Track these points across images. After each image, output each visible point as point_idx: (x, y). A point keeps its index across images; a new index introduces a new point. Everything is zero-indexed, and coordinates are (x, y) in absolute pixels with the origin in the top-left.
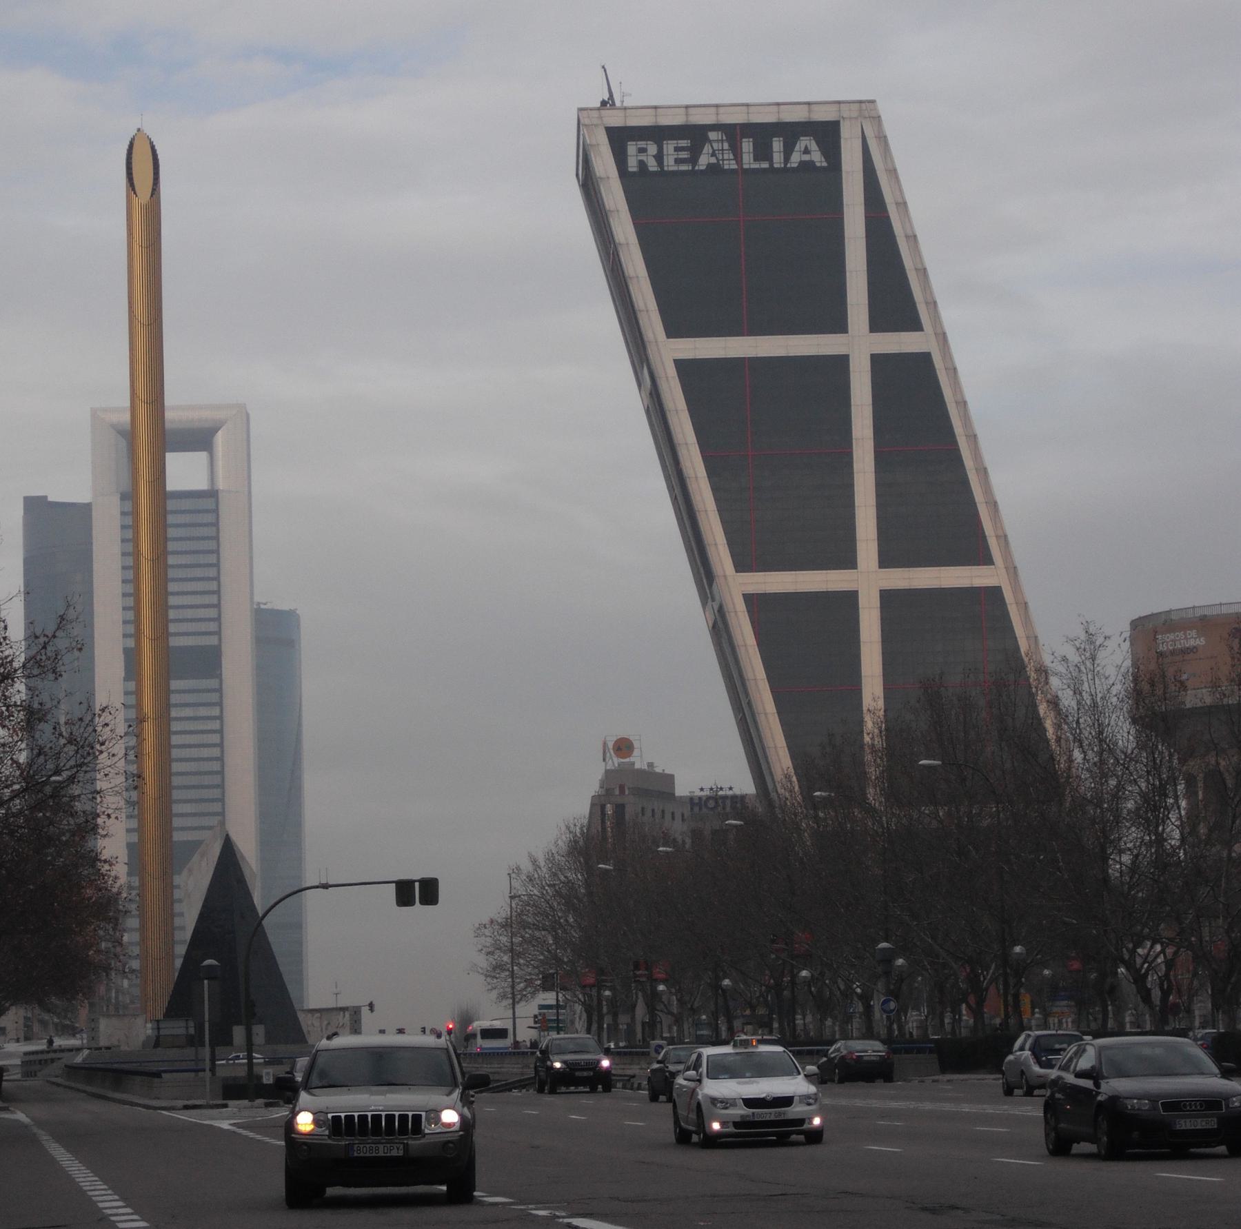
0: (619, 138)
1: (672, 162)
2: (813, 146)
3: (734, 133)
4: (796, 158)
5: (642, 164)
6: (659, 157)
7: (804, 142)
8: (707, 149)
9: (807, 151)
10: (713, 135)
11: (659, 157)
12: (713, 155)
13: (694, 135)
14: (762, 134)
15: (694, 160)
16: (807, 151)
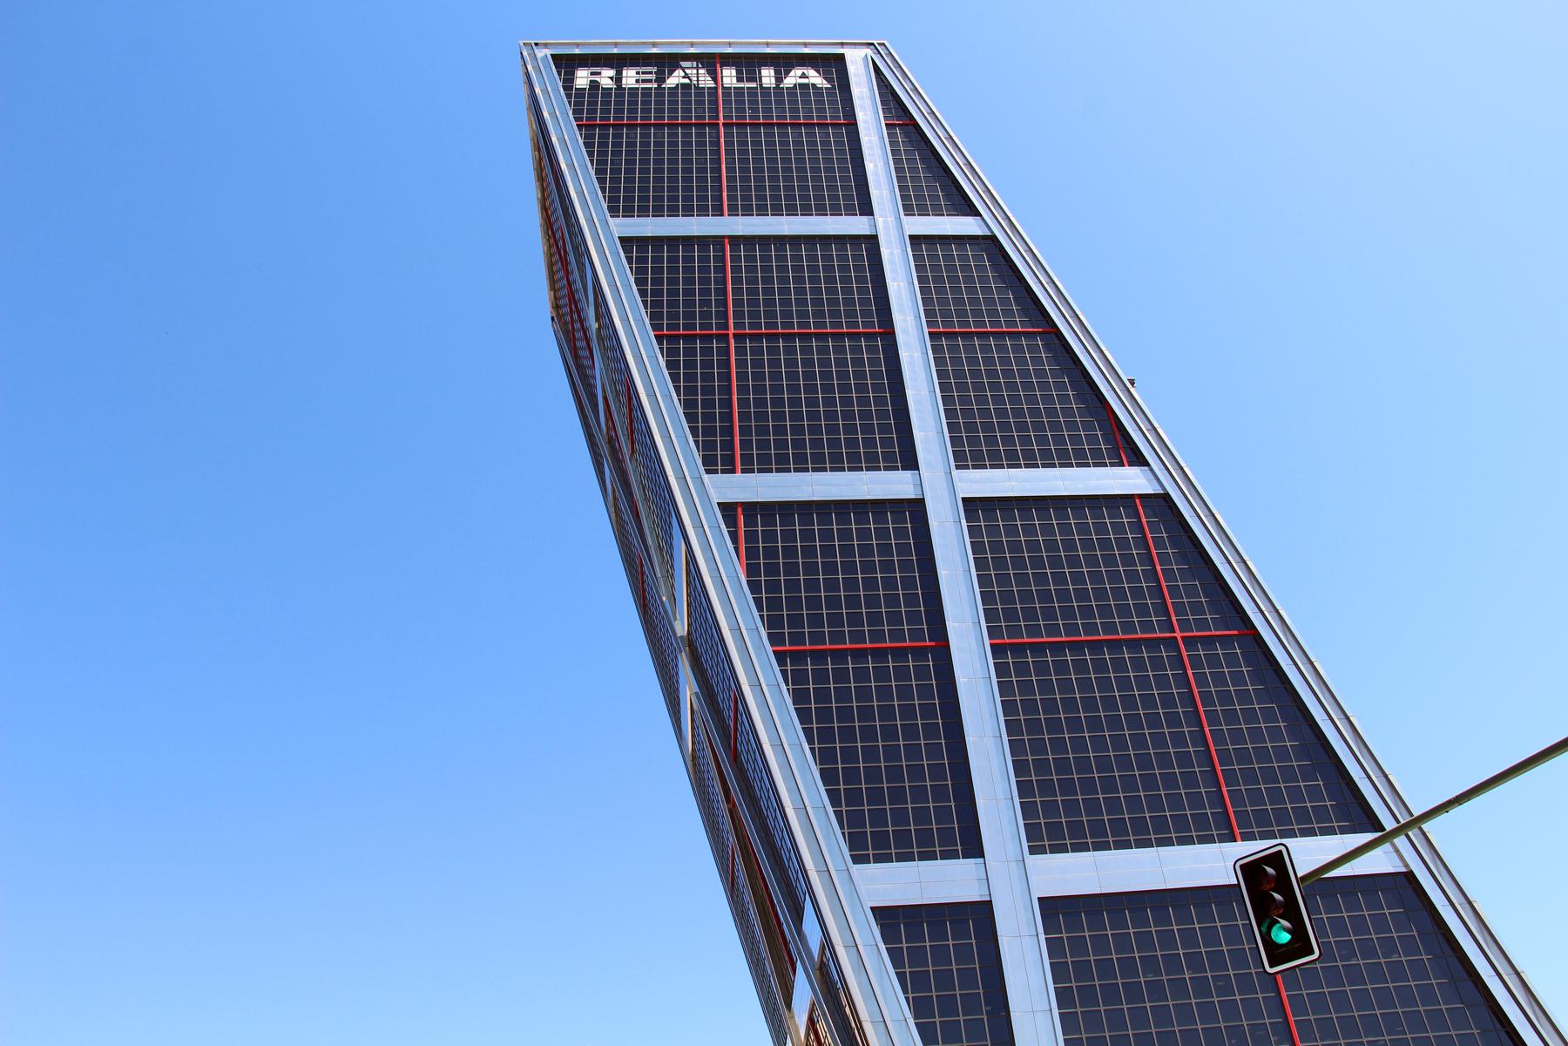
0: (566, 64)
1: (632, 81)
2: (811, 72)
3: (711, 62)
4: (790, 81)
5: (594, 86)
6: (618, 79)
7: (798, 72)
8: (679, 73)
9: (803, 76)
10: (684, 64)
11: (618, 79)
12: (686, 76)
13: (668, 62)
14: (748, 63)
15: (661, 80)
16: (803, 76)
